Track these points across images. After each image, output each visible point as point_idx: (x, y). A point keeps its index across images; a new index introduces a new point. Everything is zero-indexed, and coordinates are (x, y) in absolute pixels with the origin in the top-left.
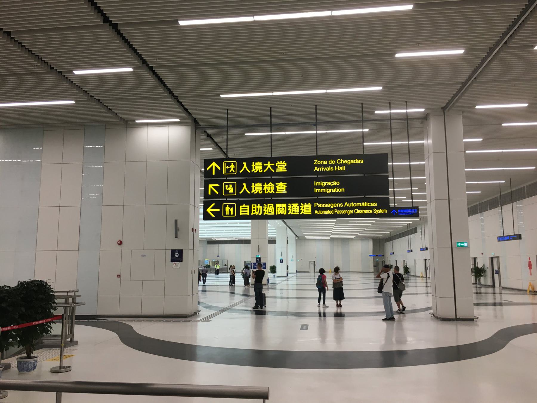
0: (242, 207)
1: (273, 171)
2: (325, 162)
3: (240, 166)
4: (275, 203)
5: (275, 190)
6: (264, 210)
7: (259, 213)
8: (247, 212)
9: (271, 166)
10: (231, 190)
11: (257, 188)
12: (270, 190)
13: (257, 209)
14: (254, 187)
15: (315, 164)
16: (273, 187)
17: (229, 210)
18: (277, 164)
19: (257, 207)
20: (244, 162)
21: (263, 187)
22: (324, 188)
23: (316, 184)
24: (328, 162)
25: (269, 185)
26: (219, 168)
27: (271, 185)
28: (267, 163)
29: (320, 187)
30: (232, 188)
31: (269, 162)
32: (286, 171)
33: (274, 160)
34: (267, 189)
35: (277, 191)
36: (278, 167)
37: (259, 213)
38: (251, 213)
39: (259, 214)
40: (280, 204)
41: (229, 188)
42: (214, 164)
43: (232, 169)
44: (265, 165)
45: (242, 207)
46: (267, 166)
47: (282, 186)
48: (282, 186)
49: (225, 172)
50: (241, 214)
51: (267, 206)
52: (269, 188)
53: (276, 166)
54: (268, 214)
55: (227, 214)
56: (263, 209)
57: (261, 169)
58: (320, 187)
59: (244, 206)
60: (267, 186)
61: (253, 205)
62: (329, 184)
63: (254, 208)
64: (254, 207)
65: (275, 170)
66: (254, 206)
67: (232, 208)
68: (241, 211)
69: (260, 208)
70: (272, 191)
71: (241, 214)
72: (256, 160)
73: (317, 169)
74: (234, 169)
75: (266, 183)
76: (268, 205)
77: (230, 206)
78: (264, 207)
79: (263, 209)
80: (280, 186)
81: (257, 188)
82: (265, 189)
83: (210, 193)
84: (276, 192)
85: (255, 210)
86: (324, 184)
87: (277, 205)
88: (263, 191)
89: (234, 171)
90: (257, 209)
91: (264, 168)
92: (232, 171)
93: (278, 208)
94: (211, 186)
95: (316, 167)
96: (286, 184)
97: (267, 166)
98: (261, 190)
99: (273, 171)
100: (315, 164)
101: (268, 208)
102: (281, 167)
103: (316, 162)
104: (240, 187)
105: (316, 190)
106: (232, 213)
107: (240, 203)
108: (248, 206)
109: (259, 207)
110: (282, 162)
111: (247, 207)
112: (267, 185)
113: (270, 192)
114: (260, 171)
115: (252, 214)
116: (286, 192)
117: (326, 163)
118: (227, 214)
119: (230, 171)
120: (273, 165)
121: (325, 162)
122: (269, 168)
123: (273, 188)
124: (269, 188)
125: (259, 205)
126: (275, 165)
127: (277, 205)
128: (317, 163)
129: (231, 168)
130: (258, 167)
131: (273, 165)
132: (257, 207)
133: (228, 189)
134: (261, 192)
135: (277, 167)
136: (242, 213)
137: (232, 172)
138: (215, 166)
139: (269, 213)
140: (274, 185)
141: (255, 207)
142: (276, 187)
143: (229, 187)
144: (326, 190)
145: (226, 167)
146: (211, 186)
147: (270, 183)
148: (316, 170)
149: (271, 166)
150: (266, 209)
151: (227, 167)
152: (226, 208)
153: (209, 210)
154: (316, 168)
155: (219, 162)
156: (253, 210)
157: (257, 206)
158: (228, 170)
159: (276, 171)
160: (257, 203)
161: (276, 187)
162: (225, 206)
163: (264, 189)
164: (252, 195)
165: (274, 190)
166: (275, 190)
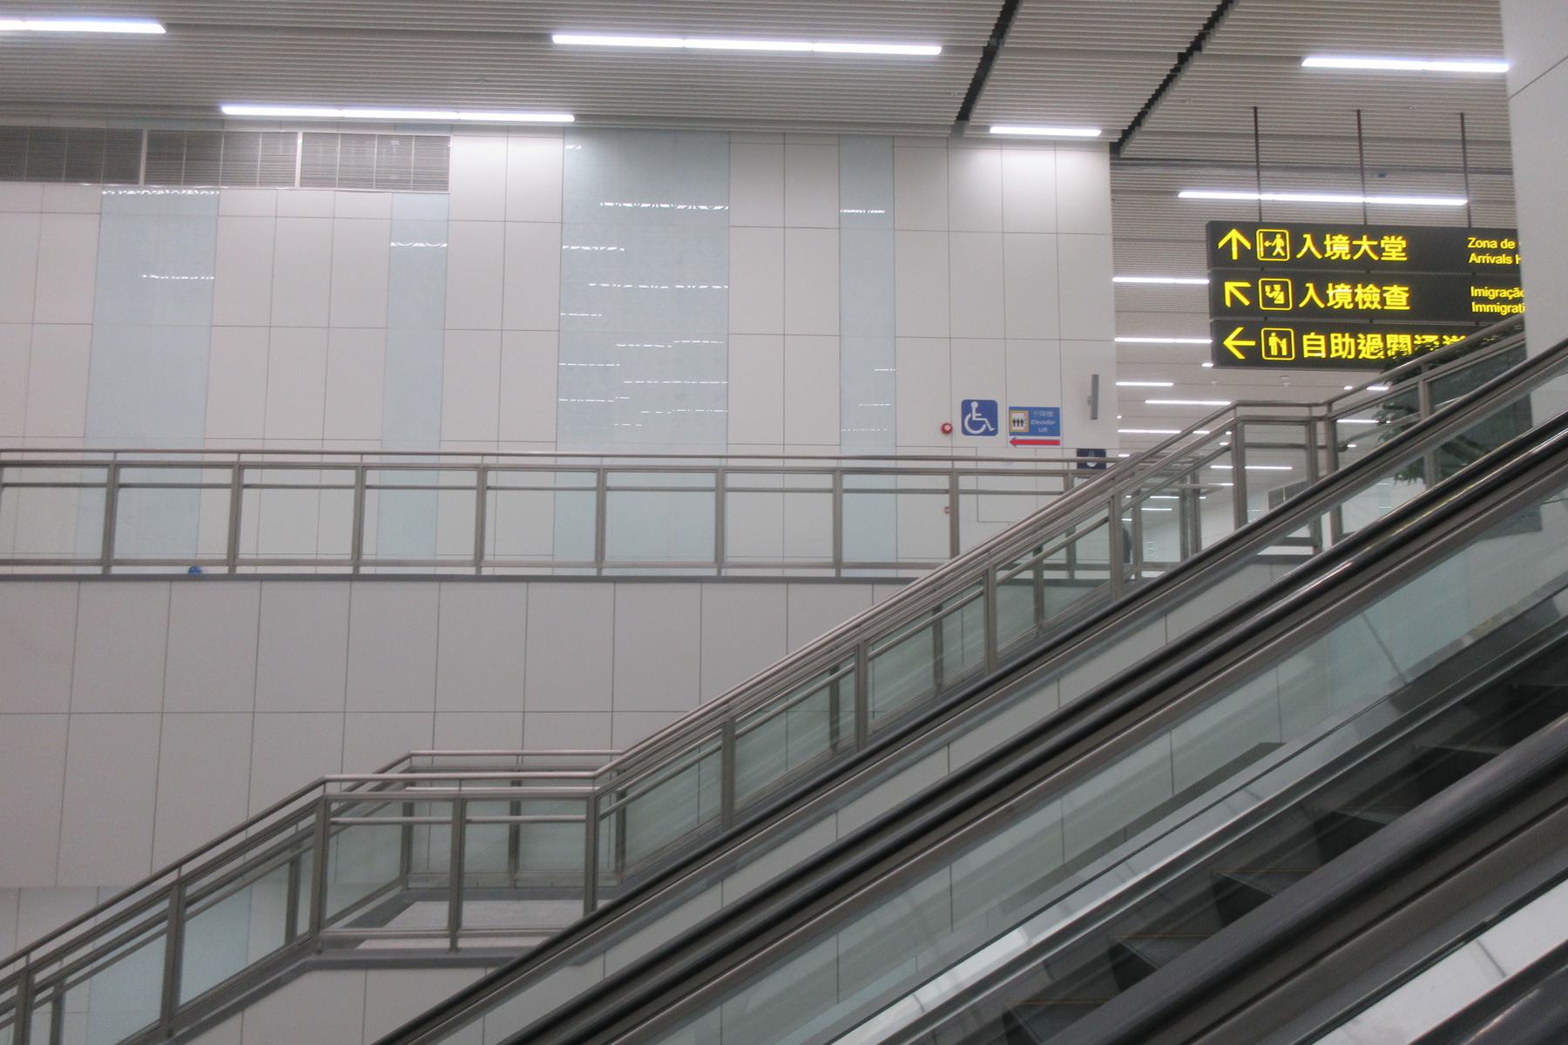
0: (1309, 340)
1: (1376, 258)
2: (1493, 245)
3: (1297, 243)
4: (1384, 331)
5: (1383, 301)
6: (1360, 347)
7: (1349, 353)
8: (1320, 352)
9: (1372, 247)
10: (1280, 299)
11: (1340, 295)
12: (1372, 303)
13: (1344, 344)
14: (1333, 292)
15: (1470, 246)
16: (1378, 295)
17: (1278, 345)
18: (1383, 242)
19: (1344, 340)
20: (1308, 233)
21: (1354, 295)
22: (1494, 302)
23: (1474, 292)
24: (1499, 245)
25: (1367, 289)
26: (1248, 245)
27: (1371, 289)
28: (1361, 239)
29: (1484, 300)
30: (1282, 293)
31: (1365, 237)
32: (1405, 259)
33: (1377, 232)
34: (1363, 299)
35: (1385, 305)
36: (1387, 249)
37: (1349, 353)
38: (1331, 353)
39: (1350, 357)
40: (1396, 336)
41: (1274, 293)
42: (1234, 235)
43: (1278, 250)
44: (1354, 243)
45: (1309, 340)
46: (1360, 246)
47: (1399, 294)
48: (1399, 294)
49: (1262, 255)
50: (1306, 355)
51: (1366, 339)
52: (1368, 296)
53: (1382, 246)
54: (1368, 356)
55: (1273, 354)
56: (1357, 344)
57: (1347, 251)
58: (1484, 300)
59: (1312, 335)
60: (1364, 293)
61: (1333, 335)
62: (1505, 293)
63: (1337, 341)
64: (1337, 339)
65: (1380, 255)
66: (1336, 338)
67: (1284, 340)
68: (1306, 349)
69: (1350, 343)
70: (1376, 306)
71: (1306, 355)
72: (1335, 229)
73: (1475, 259)
74: (1284, 248)
75: (1359, 286)
76: (1369, 336)
77: (1280, 335)
78: (1359, 341)
79: (1357, 344)
80: (1393, 294)
81: (1340, 295)
82: (1358, 298)
83: (1228, 303)
84: (1386, 308)
85: (1340, 347)
86: (1492, 294)
87: (1388, 336)
88: (1356, 304)
89: (1283, 254)
90: (1344, 344)
91: (1354, 249)
92: (1278, 254)
93: (1392, 344)
94: (1230, 287)
95: (1473, 255)
96: (1406, 289)
97: (1360, 246)
98: (1350, 300)
99: (1376, 258)
100: (1470, 246)
101: (1368, 344)
102: (1395, 249)
103: (1473, 243)
104: (1300, 293)
105: (1476, 308)
106: (1284, 352)
107: (1301, 330)
108: (1322, 338)
109: (1347, 339)
110: (1396, 239)
111: (1319, 340)
112: (1362, 290)
113: (1370, 306)
114: (1344, 258)
115: (1333, 355)
116: (1408, 308)
117: (1496, 247)
118: (1273, 354)
119: (1275, 254)
120: (1375, 243)
121: (1493, 245)
122: (1365, 251)
123: (1377, 298)
124: (1368, 296)
125: (1347, 335)
126: (1379, 244)
127: (1388, 336)
128: (1474, 244)
129: (1275, 247)
130: (1338, 247)
131: (1375, 243)
132: (1344, 340)
133: (1270, 296)
134: (1351, 306)
135: (1384, 248)
136: (1310, 351)
137: (1279, 255)
138: (1238, 241)
139: (1372, 354)
140: (1379, 291)
141: (1340, 341)
142: (1385, 295)
143: (1272, 290)
144: (1498, 308)
145: (1264, 242)
146: (1230, 287)
147: (1371, 286)
148: (1474, 261)
149: (1372, 247)
150: (1365, 345)
151: (1267, 244)
152: (1270, 339)
153: (1230, 343)
154: (1473, 258)
155: (1248, 229)
156: (1333, 348)
157: (1343, 336)
158: (1269, 251)
159: (1383, 259)
160: (1342, 329)
161: (1385, 295)
162: (1268, 334)
163: (1356, 300)
164: (1329, 311)
165: (1379, 303)
166: (1383, 301)
